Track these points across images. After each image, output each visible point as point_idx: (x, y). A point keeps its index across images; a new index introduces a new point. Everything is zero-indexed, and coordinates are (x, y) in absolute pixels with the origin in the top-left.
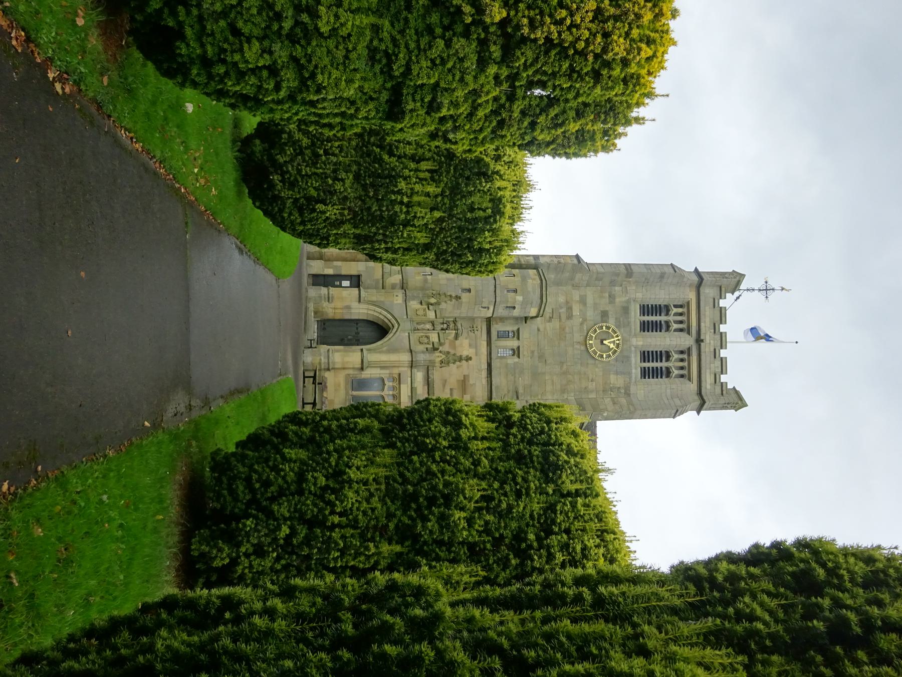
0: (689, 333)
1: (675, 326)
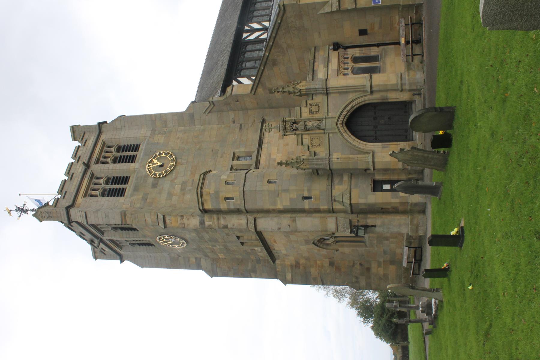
0: (92, 175)
1: (101, 181)
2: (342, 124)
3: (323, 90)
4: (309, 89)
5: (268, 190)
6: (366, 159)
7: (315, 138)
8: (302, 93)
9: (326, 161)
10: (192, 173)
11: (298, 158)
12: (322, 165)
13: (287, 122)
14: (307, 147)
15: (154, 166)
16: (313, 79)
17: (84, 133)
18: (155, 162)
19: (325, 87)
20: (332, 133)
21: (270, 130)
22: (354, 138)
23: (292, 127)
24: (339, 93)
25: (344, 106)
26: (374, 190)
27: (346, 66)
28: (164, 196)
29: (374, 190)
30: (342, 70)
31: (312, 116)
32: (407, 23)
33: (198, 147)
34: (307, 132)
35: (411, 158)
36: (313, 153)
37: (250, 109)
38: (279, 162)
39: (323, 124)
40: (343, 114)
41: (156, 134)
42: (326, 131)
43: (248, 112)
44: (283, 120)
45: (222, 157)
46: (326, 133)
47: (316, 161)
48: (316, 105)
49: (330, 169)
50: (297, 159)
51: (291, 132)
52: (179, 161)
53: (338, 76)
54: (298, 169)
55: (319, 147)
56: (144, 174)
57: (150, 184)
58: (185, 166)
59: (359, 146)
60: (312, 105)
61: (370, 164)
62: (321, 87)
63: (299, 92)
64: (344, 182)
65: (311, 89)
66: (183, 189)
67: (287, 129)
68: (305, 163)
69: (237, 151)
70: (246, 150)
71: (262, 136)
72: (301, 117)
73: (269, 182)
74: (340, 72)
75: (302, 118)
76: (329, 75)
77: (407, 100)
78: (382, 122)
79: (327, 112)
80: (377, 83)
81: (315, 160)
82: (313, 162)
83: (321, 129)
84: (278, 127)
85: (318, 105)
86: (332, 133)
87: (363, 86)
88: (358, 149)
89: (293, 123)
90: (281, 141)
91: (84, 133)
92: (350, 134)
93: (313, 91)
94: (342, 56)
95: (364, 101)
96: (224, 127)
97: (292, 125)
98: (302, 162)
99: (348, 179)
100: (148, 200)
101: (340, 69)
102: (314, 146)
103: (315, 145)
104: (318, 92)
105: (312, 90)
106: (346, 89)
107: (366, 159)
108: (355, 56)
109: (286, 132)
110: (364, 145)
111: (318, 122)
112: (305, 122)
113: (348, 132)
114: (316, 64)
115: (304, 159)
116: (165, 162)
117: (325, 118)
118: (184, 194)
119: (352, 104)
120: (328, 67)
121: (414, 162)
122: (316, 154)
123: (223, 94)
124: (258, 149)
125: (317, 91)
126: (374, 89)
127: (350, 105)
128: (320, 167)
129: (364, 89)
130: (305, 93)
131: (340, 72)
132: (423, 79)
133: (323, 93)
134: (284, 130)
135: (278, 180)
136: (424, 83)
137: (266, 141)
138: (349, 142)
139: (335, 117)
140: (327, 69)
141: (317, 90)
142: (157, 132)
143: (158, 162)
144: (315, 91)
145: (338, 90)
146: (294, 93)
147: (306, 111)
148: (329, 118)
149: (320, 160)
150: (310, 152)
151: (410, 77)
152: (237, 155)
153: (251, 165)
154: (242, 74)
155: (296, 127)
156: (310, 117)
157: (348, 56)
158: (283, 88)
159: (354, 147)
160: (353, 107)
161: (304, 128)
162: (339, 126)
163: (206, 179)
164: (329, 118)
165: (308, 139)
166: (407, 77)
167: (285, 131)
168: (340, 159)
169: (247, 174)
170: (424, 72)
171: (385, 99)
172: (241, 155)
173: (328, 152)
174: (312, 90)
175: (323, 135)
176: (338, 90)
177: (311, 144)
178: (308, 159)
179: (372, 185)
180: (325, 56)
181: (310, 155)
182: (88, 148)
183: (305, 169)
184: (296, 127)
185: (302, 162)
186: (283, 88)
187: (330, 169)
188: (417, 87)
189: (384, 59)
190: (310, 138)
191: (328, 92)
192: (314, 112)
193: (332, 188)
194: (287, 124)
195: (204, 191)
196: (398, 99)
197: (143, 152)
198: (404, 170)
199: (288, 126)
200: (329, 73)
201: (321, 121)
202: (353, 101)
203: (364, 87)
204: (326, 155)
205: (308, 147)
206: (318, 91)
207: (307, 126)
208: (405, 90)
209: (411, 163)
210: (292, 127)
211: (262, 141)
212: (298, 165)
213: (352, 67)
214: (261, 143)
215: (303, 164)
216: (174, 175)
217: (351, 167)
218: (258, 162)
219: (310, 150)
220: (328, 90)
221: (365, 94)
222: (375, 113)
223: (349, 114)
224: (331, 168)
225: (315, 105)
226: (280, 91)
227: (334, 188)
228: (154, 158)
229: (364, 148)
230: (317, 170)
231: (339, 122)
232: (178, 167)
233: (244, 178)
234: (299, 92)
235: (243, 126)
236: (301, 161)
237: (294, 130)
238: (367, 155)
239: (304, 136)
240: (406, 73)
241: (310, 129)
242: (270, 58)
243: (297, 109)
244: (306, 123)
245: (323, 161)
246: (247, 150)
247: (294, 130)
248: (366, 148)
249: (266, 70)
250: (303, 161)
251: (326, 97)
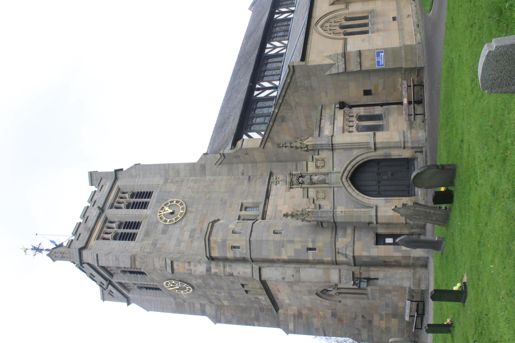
0: (106, 219)
1: (114, 225)
2: (346, 179)
3: (329, 145)
4: (316, 145)
5: (273, 240)
6: (369, 213)
7: (320, 191)
8: (309, 148)
9: (330, 214)
10: (201, 221)
11: (303, 210)
12: (327, 218)
13: (293, 176)
14: (312, 200)
15: (165, 213)
16: (319, 136)
17: (101, 179)
18: (166, 210)
19: (331, 143)
20: (337, 187)
21: (278, 182)
22: (358, 192)
23: (298, 180)
24: (343, 149)
25: (348, 162)
26: (377, 243)
27: (351, 124)
28: (173, 242)
29: (377, 243)
30: (348, 128)
31: (318, 171)
32: (409, 85)
33: (208, 196)
34: (312, 186)
35: (413, 213)
36: (318, 206)
37: (259, 162)
38: (285, 213)
39: (328, 178)
40: (347, 169)
41: (169, 183)
43: (256, 165)
44: (290, 173)
45: (230, 207)
46: (331, 187)
47: (321, 214)
48: (322, 160)
49: (334, 222)
50: (303, 211)
51: (297, 185)
52: (189, 209)
53: (343, 133)
54: (303, 221)
56: (155, 220)
57: (161, 230)
58: (195, 214)
59: (363, 201)
61: (373, 218)
62: (326, 143)
63: (306, 147)
64: (347, 235)
65: (317, 145)
66: (191, 237)
67: (293, 182)
68: (310, 215)
69: (244, 201)
70: (253, 201)
71: (270, 188)
72: (307, 171)
73: (275, 232)
74: (345, 130)
75: (308, 172)
76: (334, 132)
77: (409, 157)
78: (386, 178)
79: (332, 166)
80: (381, 141)
81: (320, 213)
82: (318, 214)
83: (326, 183)
84: (285, 180)
85: (324, 160)
86: (337, 187)
87: (367, 143)
88: (362, 203)
89: (300, 177)
90: (288, 194)
91: (101, 179)
92: (354, 188)
93: (319, 147)
94: (348, 115)
95: (368, 157)
96: (233, 178)
97: (298, 178)
99: (352, 232)
100: (158, 246)
101: (345, 127)
102: (319, 199)
103: (320, 199)
104: (324, 148)
105: (318, 146)
106: (351, 146)
107: (369, 213)
108: (359, 114)
109: (293, 185)
110: (368, 200)
111: (323, 177)
112: (311, 176)
113: (352, 186)
114: (322, 121)
115: (309, 212)
116: (176, 209)
117: (331, 173)
118: (192, 242)
119: (356, 160)
120: (334, 124)
121: (416, 217)
123: (233, 147)
124: (265, 201)
125: (323, 146)
126: (377, 146)
127: (355, 161)
128: (325, 219)
129: (368, 146)
130: (311, 148)
131: (345, 130)
132: (425, 138)
133: (329, 149)
134: (290, 183)
135: (283, 231)
136: (426, 141)
137: (272, 193)
138: (353, 197)
139: (340, 172)
140: (333, 126)
141: (323, 145)
142: (169, 181)
143: (169, 210)
144: (321, 147)
145: (343, 146)
146: (301, 148)
147: (312, 166)
148: (334, 173)
149: (324, 213)
150: (315, 205)
151: (412, 135)
152: (245, 205)
153: (258, 215)
154: (252, 128)
155: (302, 181)
157: (353, 114)
158: (291, 143)
159: (357, 201)
160: (357, 163)
163: (214, 227)
164: (334, 173)
166: (409, 136)
167: (292, 184)
168: (344, 213)
169: (254, 224)
170: (425, 131)
171: (387, 156)
172: (248, 206)
173: (333, 205)
174: (318, 146)
175: (328, 189)
176: (343, 146)
177: (316, 197)
178: (312, 212)
179: (375, 239)
180: (331, 114)
181: (315, 208)
182: (104, 193)
183: (310, 221)
184: (302, 181)
185: (307, 214)
186: (291, 143)
187: (334, 222)
188: (419, 145)
189: (387, 118)
191: (333, 148)
192: (319, 167)
193: (336, 240)
194: (293, 178)
195: (211, 239)
196: (401, 156)
197: (155, 199)
198: (407, 224)
199: (295, 179)
200: (335, 130)
201: (326, 176)
202: (357, 157)
203: (368, 144)
204: (331, 208)
205: (314, 200)
206: (324, 146)
208: (408, 147)
209: (413, 218)
210: (298, 180)
211: (269, 193)
212: (303, 217)
213: (357, 125)
214: (268, 195)
215: (308, 217)
216: (183, 222)
217: (355, 221)
218: (265, 213)
219: (315, 203)
220: (333, 146)
221: (369, 151)
222: (378, 169)
223: (353, 169)
224: (335, 221)
225: (321, 160)
226: (288, 146)
227: (338, 240)
228: (165, 205)
229: (367, 202)
230: (322, 223)
231: (344, 177)
232: (188, 215)
233: (251, 228)
234: (306, 147)
235: (251, 177)
236: (306, 213)
237: (300, 183)
238: (371, 210)
239: (310, 190)
240: (409, 131)
241: (316, 183)
242: (279, 114)
243: (303, 164)
244: (312, 177)
245: (327, 214)
246: (255, 201)
247: (300, 183)
248: (369, 202)
249: (275, 125)
250: (308, 213)
251: (332, 152)
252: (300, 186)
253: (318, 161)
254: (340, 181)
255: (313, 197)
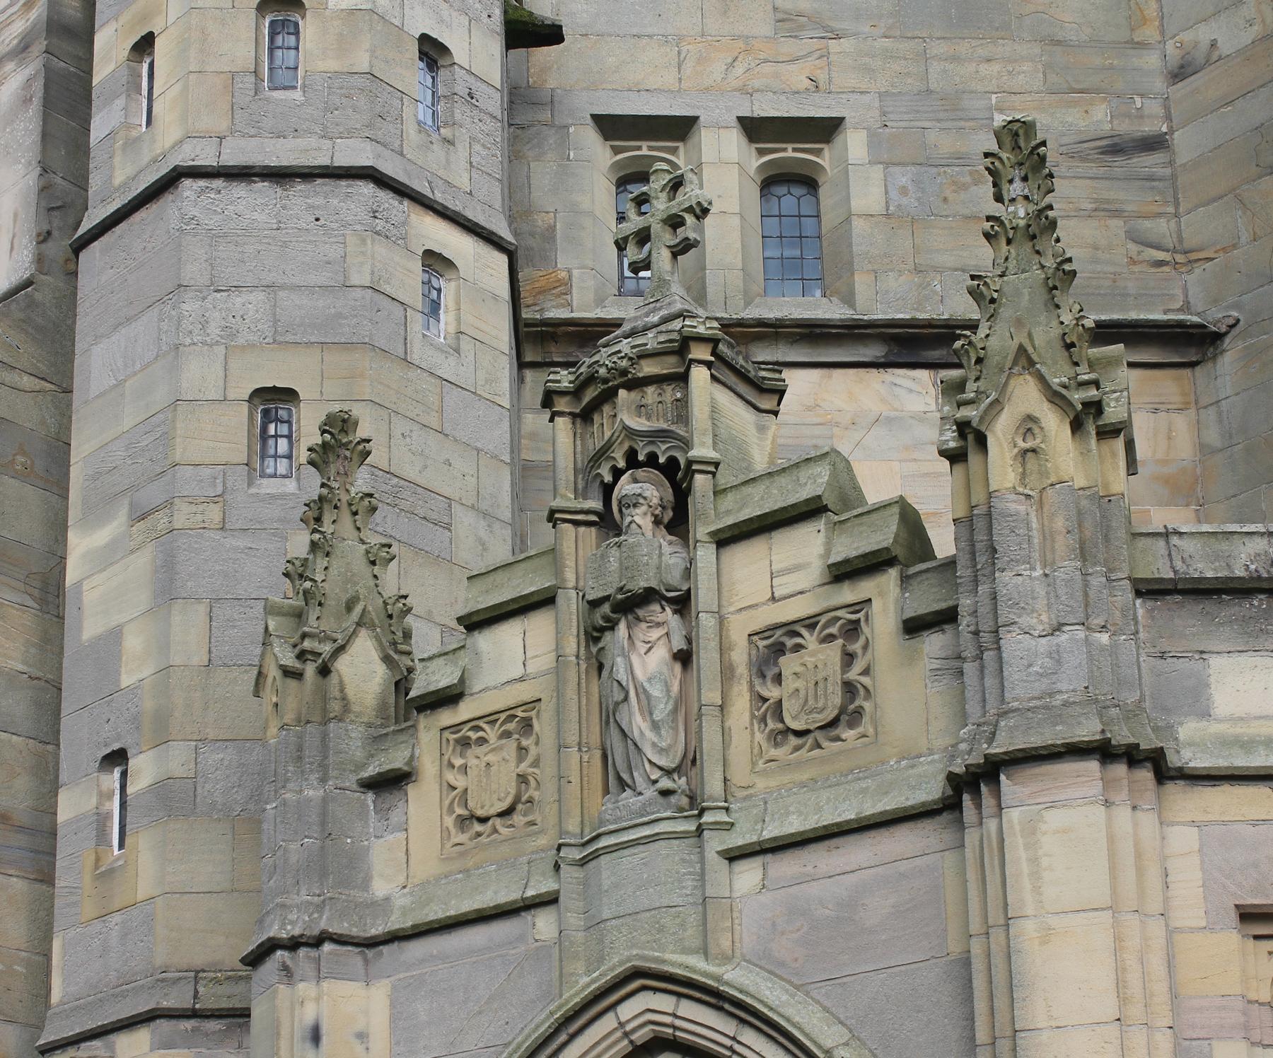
23: (632, 460)
34: (571, 645)
38: (361, 433)
39: (642, 812)
42: (583, 862)
48: (850, 688)
55: (449, 821)
60: (856, 647)
79: (771, 831)
97: (652, 460)
98: (302, 656)
102: (458, 762)
103: (464, 769)
117: (700, 831)
122: (390, 798)
156: (724, 648)
161: (595, 604)
162: (627, 1010)
165: (521, 679)
190: (525, 692)
192: (778, 679)
207: (622, 626)
210: (632, 460)
231: (664, 1002)
239: (539, 626)
250: (310, 669)
252: (567, 500)
253: (832, 653)
254: (614, 965)
255: (476, 685)
